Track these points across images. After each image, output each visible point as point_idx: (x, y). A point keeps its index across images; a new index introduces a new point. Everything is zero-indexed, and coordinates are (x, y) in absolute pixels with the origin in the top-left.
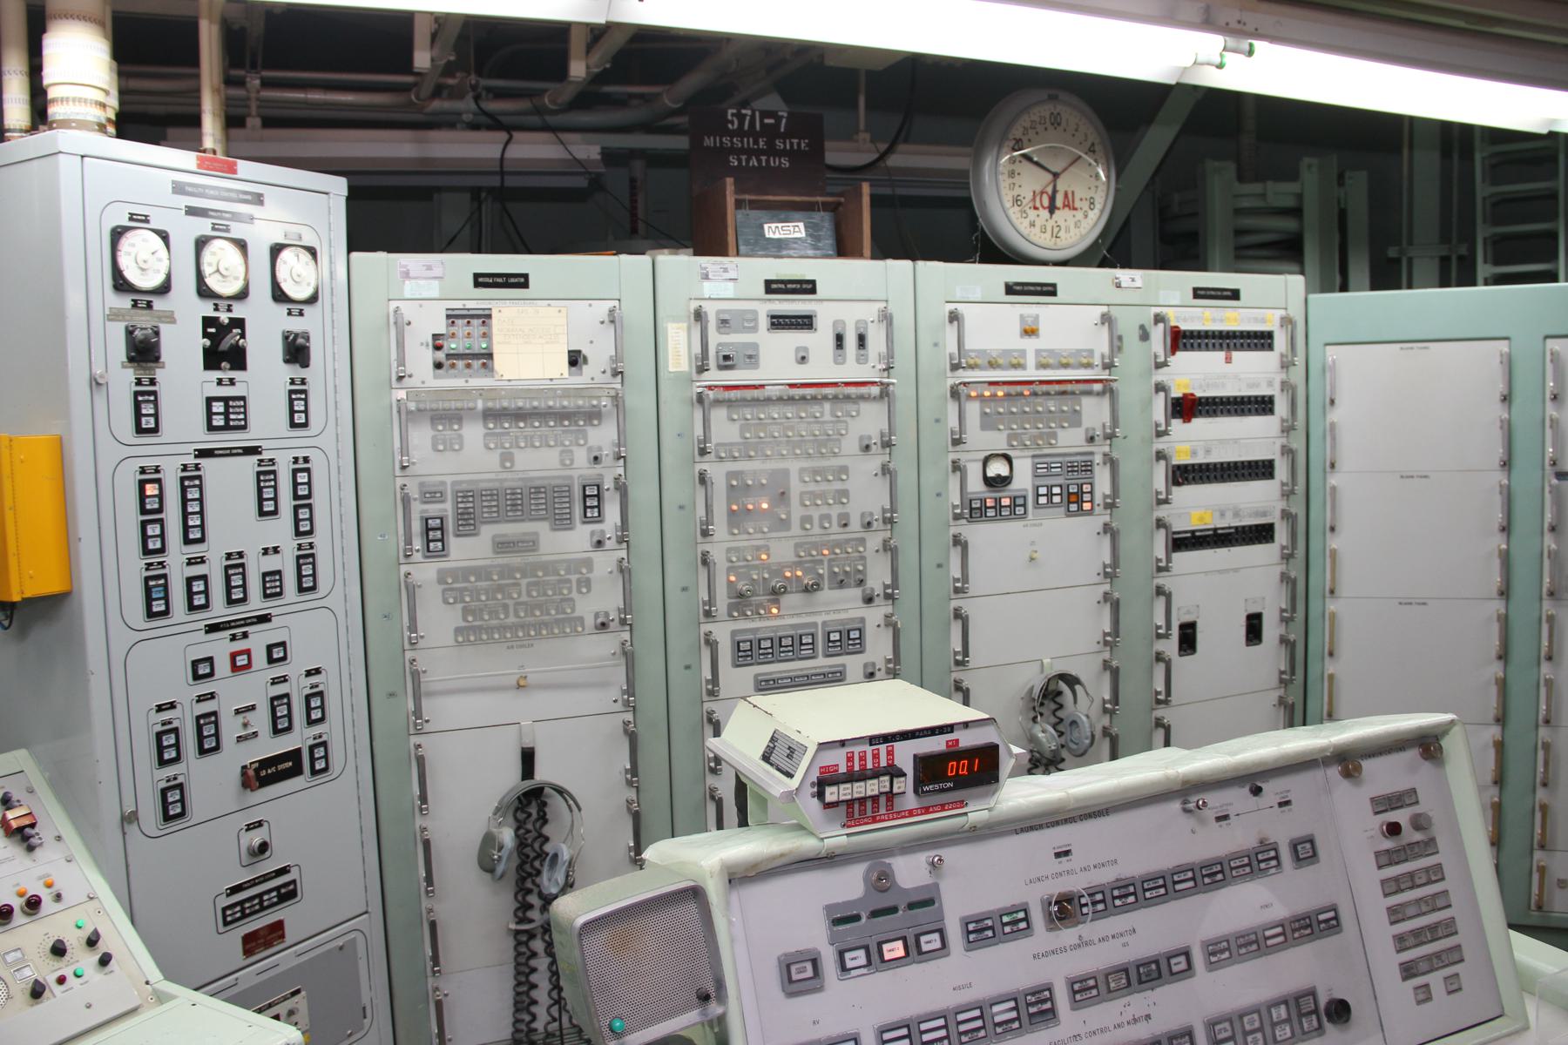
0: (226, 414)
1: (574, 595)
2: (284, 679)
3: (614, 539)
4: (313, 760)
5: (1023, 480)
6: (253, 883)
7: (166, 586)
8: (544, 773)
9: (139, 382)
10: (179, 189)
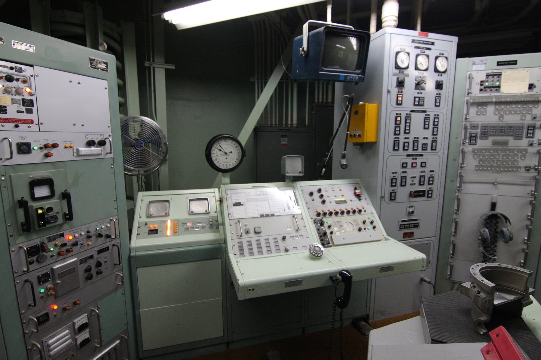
0: (419, 101)
1: (519, 159)
2: (424, 172)
3: (537, 144)
4: (428, 194)
6: (408, 221)
7: (399, 143)
8: (499, 210)
9: (398, 92)
10: (413, 41)
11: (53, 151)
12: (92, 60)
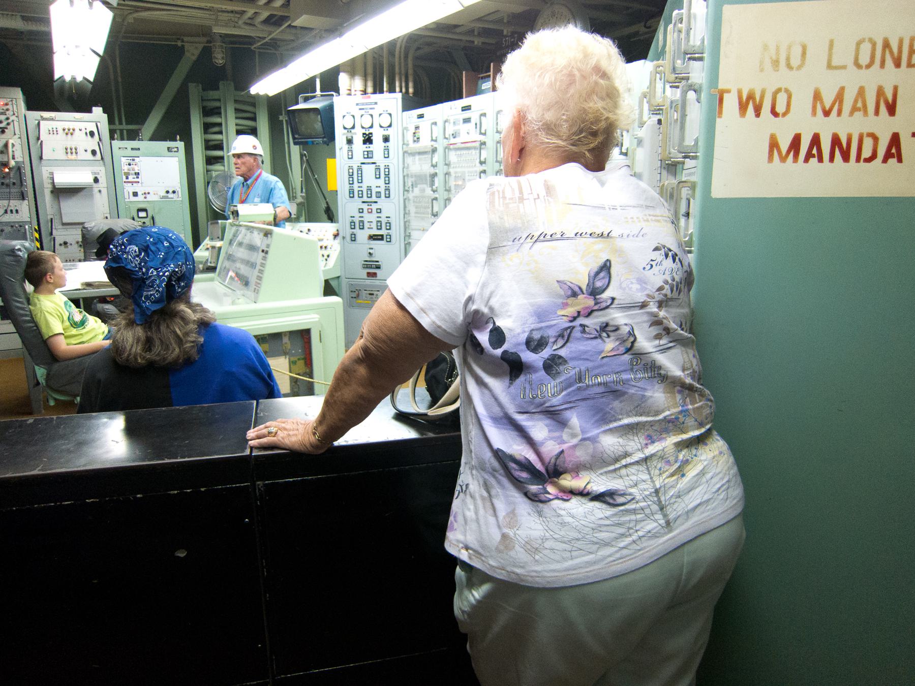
11: (148, 196)
12: (168, 148)
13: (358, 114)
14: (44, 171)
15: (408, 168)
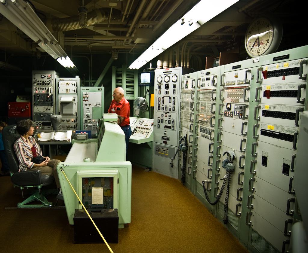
5: (233, 109)
10: (164, 72)
11: (90, 105)
13: (163, 76)
14: (59, 96)
15: (183, 99)
